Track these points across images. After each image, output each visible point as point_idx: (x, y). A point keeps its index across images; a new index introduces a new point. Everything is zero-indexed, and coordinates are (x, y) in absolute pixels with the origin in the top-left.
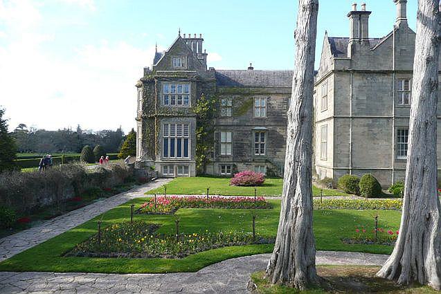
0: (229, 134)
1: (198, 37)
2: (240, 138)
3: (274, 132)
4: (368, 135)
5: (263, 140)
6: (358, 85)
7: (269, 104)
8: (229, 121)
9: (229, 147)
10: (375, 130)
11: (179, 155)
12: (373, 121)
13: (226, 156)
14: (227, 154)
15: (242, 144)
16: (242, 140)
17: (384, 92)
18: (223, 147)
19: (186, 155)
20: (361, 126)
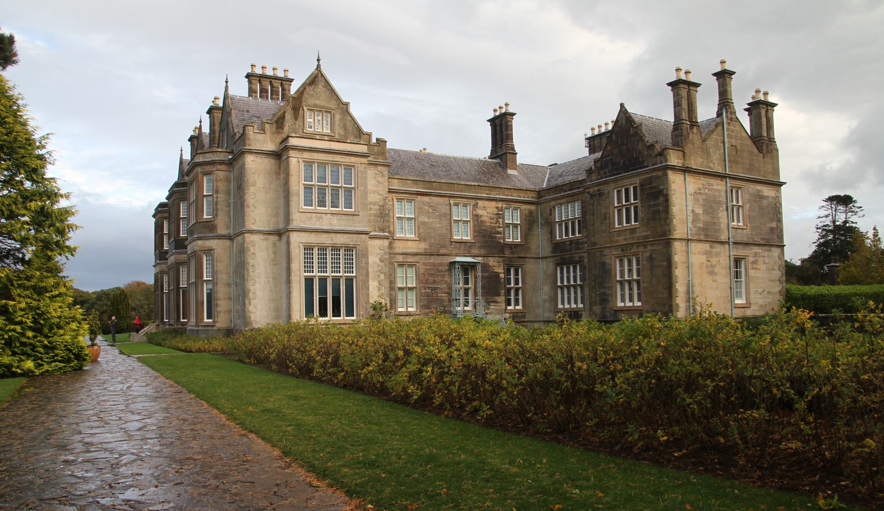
0: (411, 273)
1: (281, 74)
2: (431, 279)
3: (485, 267)
4: (707, 267)
5: (466, 282)
6: (693, 192)
7: (476, 217)
8: (413, 247)
9: (412, 296)
10: (714, 260)
11: (337, 313)
12: (711, 247)
13: (409, 314)
14: (409, 309)
15: (435, 289)
16: (434, 282)
17: (719, 203)
18: (400, 296)
19: (350, 313)
20: (699, 253)
